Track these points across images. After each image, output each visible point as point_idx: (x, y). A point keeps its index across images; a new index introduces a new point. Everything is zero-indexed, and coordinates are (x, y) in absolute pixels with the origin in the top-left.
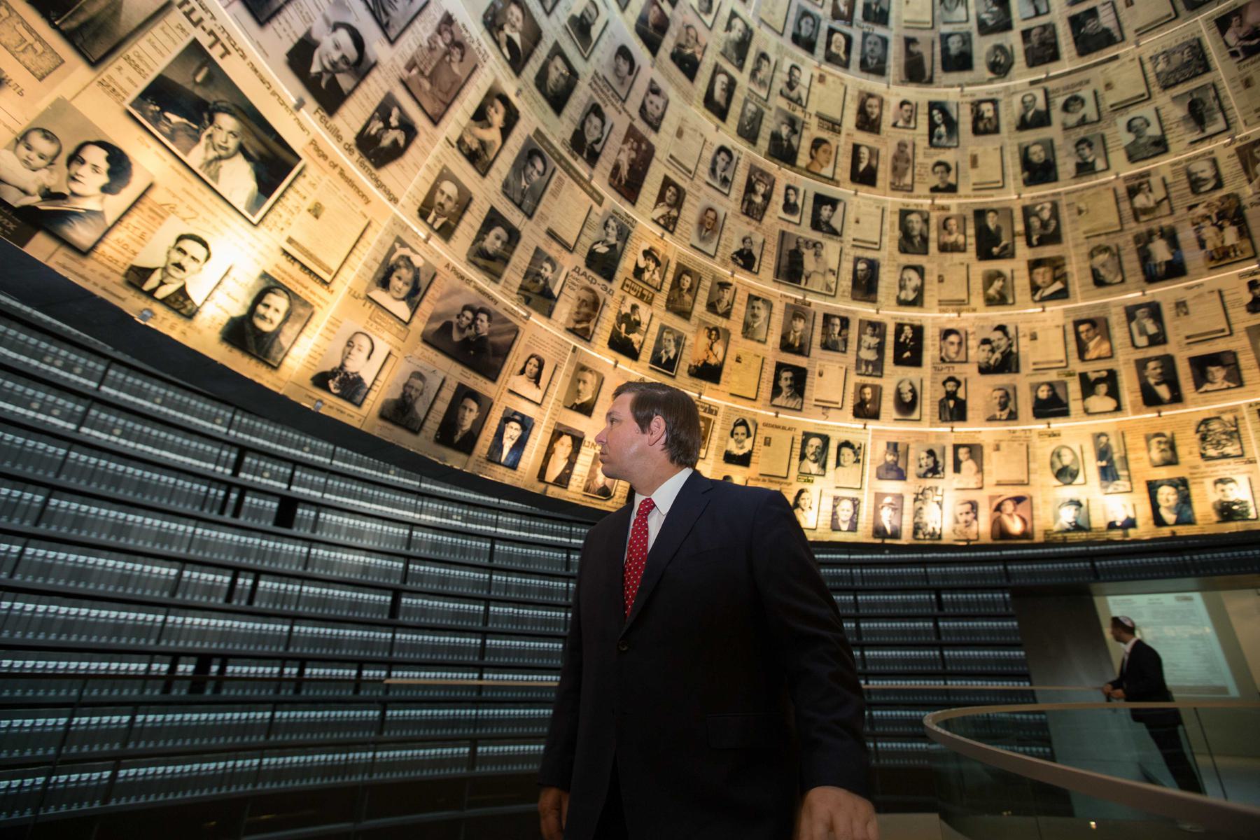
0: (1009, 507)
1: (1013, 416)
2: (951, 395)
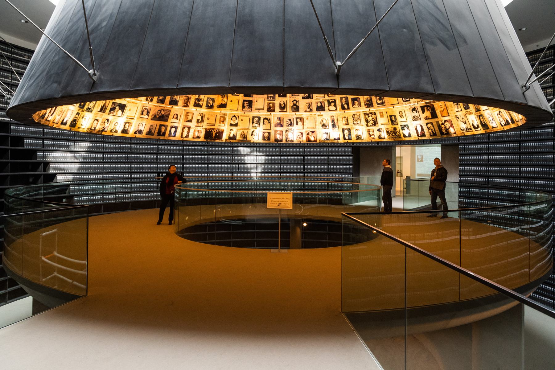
0: (310, 134)
1: (311, 110)
2: (295, 105)
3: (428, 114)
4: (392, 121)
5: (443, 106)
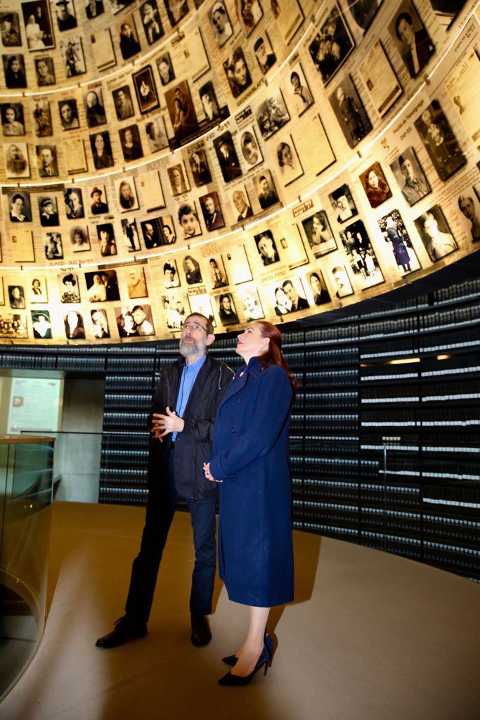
3: (99, 290)
4: (12, 299)
5: (138, 276)
